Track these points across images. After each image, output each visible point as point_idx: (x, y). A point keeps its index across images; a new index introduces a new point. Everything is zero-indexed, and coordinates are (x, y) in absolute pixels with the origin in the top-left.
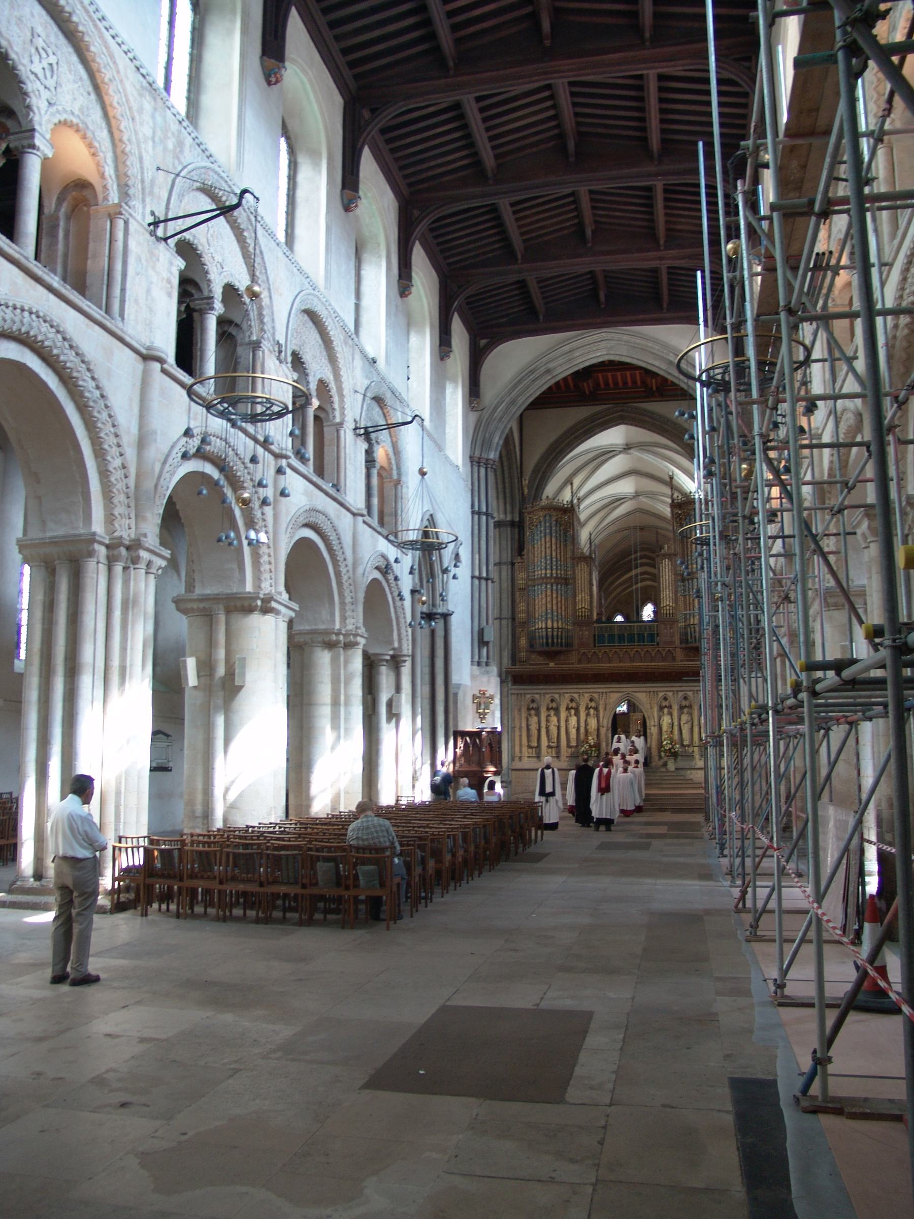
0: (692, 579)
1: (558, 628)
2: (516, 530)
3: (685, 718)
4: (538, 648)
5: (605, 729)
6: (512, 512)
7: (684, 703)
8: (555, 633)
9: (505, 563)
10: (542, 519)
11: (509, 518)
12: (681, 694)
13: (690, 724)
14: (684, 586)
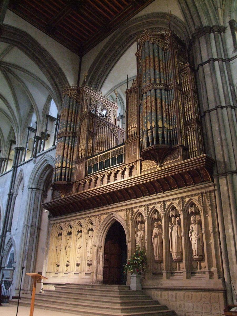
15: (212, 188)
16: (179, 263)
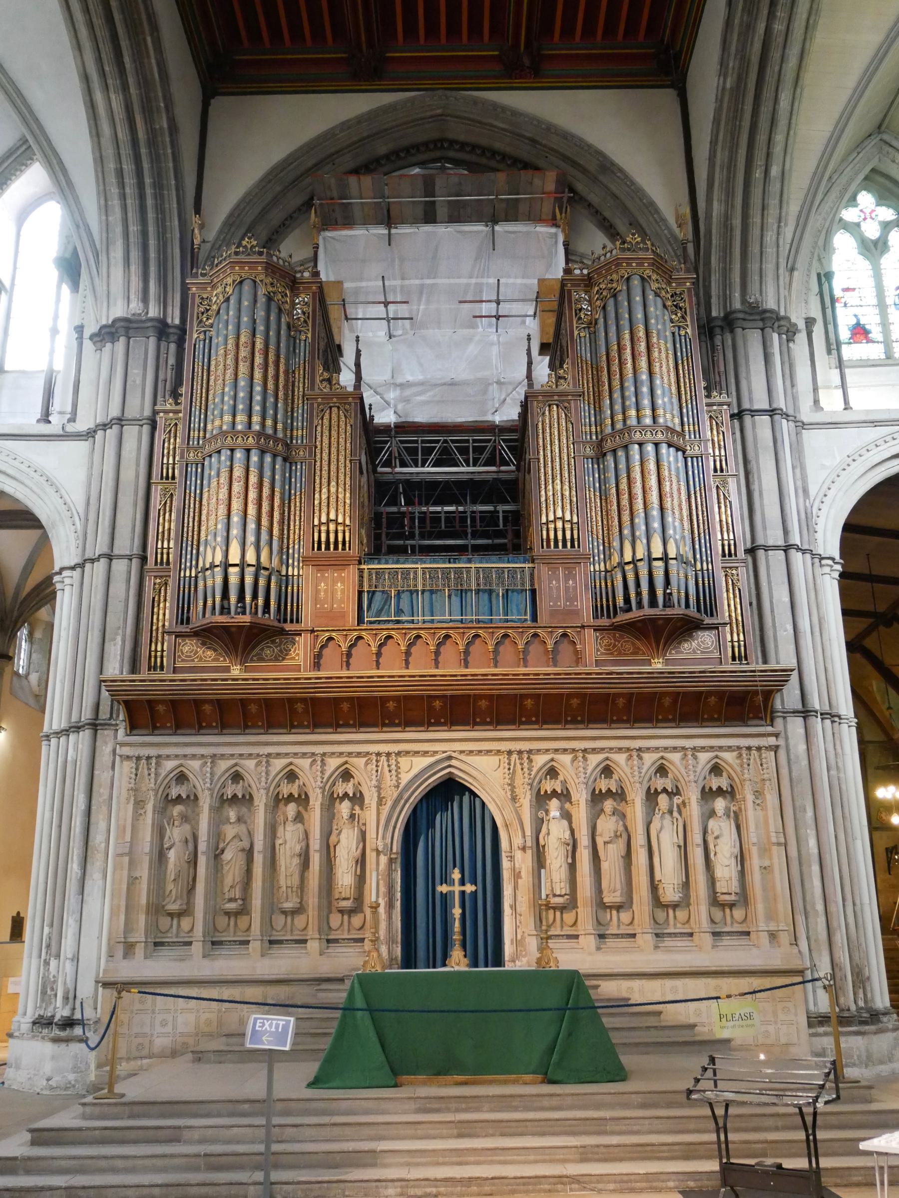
0: (626, 447)
1: (259, 567)
2: (173, 347)
3: (607, 825)
4: (198, 620)
5: (383, 859)
6: (164, 302)
7: (603, 785)
8: (249, 580)
9: (133, 421)
10: (229, 289)
11: (153, 312)
12: (594, 760)
13: (621, 844)
14: (603, 471)
15: (772, 741)
16: (674, 911)
